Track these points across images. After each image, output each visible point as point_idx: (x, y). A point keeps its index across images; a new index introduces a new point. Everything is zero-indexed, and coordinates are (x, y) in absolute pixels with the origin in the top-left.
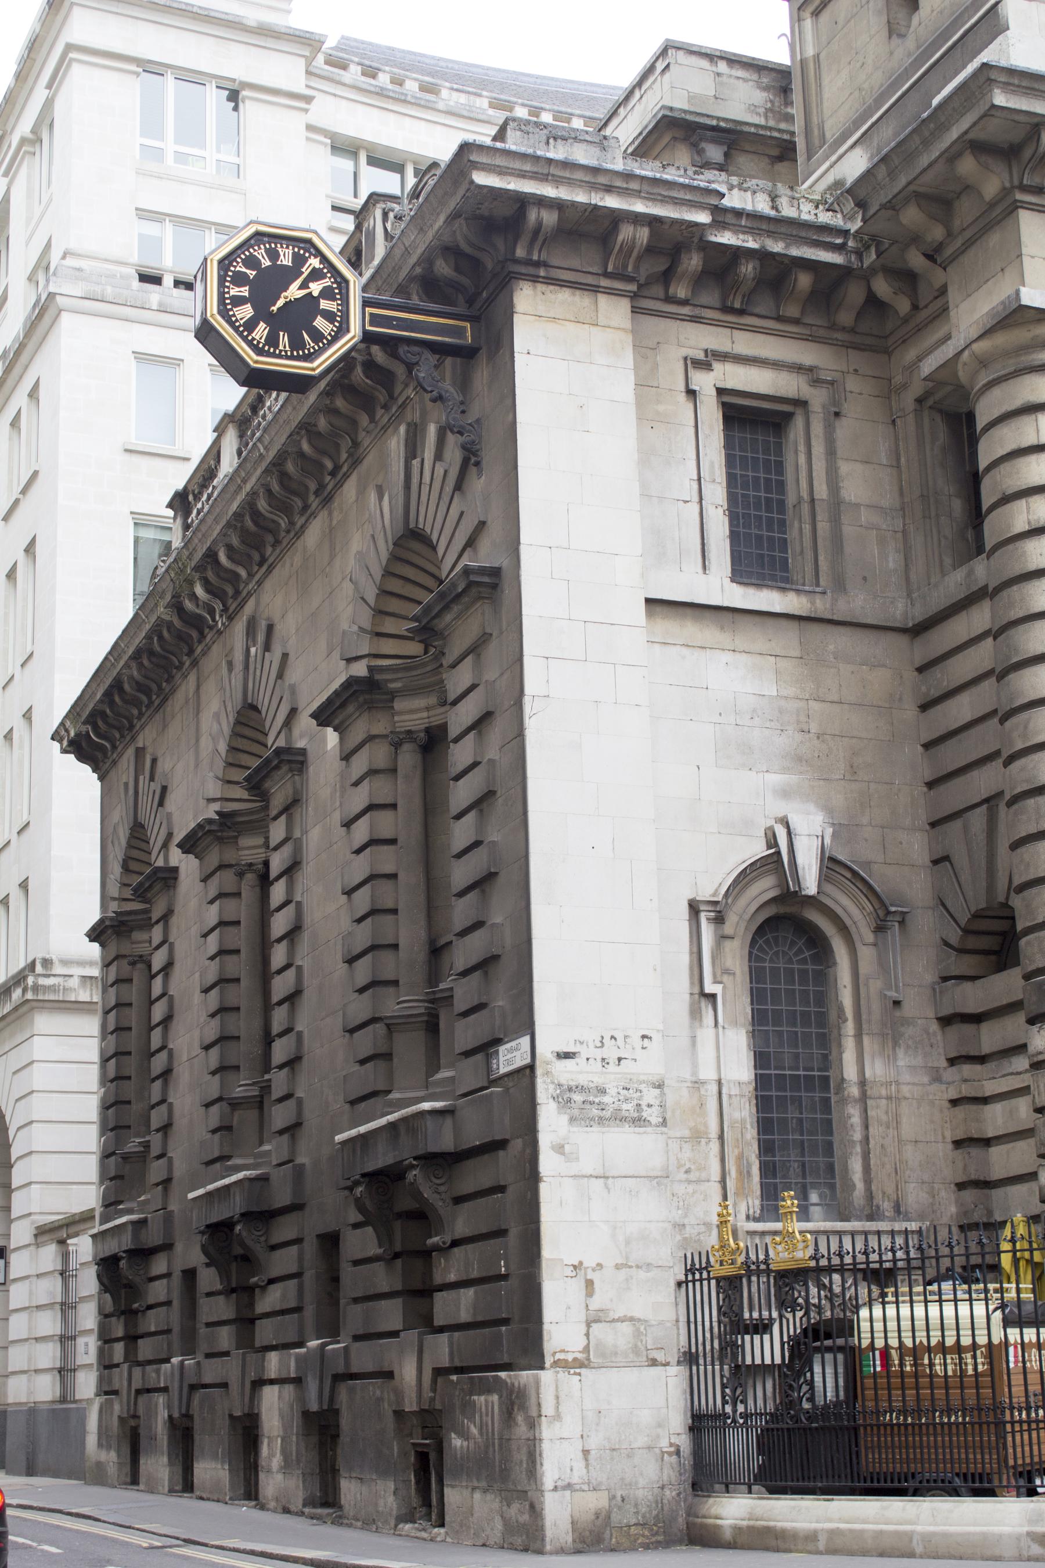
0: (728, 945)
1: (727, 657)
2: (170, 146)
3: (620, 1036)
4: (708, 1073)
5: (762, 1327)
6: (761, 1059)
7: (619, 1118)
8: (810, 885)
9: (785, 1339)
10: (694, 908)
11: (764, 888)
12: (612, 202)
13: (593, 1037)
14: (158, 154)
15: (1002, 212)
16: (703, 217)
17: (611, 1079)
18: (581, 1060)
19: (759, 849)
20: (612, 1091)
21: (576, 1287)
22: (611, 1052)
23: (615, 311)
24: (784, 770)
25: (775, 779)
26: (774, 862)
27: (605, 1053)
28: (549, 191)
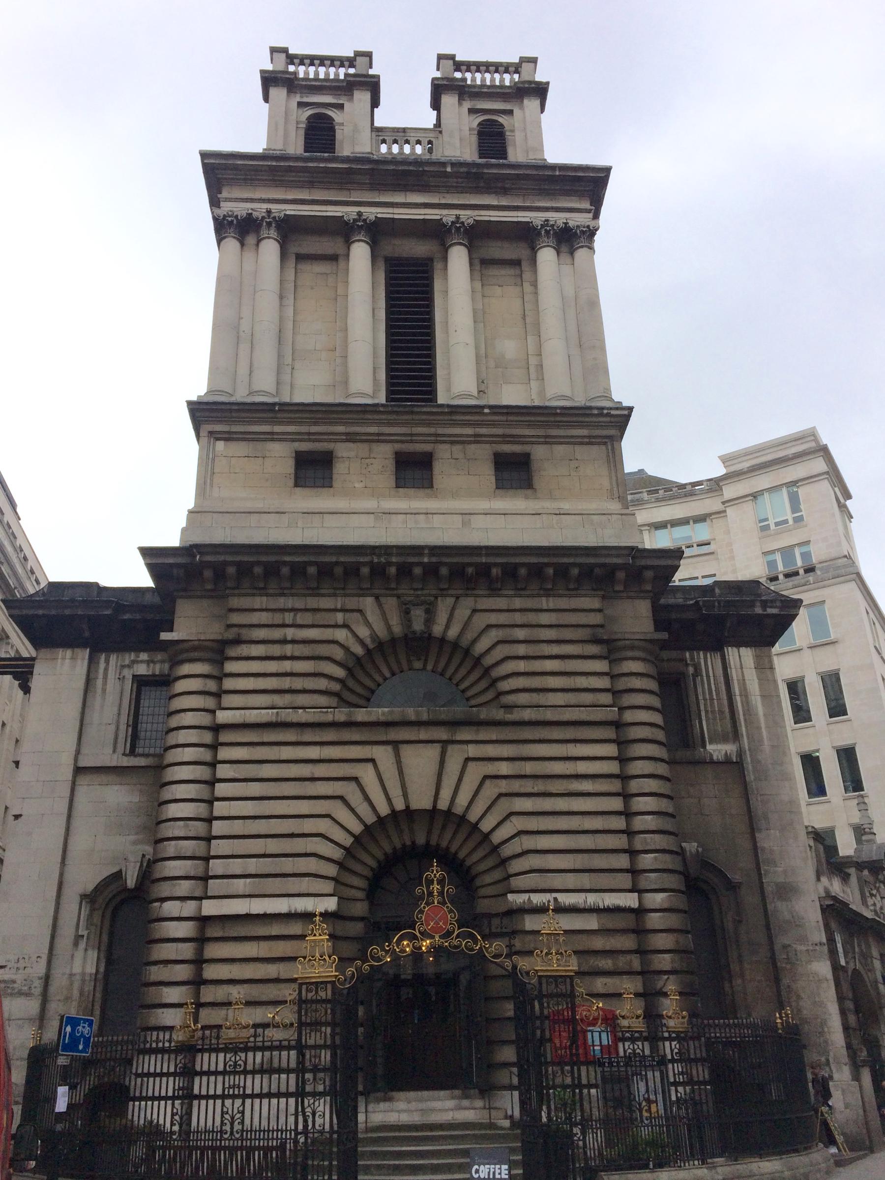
0: (96, 912)
1: (116, 788)
3: (26, 957)
9: (177, 1088)
11: (114, 888)
12: (67, 612)
13: (13, 958)
15: (174, 602)
16: (108, 612)
17: (19, 977)
18: (7, 969)
19: (115, 870)
20: (19, 982)
22: (21, 964)
24: (137, 834)
25: (132, 838)
26: (118, 876)
27: (19, 965)
28: (40, 612)
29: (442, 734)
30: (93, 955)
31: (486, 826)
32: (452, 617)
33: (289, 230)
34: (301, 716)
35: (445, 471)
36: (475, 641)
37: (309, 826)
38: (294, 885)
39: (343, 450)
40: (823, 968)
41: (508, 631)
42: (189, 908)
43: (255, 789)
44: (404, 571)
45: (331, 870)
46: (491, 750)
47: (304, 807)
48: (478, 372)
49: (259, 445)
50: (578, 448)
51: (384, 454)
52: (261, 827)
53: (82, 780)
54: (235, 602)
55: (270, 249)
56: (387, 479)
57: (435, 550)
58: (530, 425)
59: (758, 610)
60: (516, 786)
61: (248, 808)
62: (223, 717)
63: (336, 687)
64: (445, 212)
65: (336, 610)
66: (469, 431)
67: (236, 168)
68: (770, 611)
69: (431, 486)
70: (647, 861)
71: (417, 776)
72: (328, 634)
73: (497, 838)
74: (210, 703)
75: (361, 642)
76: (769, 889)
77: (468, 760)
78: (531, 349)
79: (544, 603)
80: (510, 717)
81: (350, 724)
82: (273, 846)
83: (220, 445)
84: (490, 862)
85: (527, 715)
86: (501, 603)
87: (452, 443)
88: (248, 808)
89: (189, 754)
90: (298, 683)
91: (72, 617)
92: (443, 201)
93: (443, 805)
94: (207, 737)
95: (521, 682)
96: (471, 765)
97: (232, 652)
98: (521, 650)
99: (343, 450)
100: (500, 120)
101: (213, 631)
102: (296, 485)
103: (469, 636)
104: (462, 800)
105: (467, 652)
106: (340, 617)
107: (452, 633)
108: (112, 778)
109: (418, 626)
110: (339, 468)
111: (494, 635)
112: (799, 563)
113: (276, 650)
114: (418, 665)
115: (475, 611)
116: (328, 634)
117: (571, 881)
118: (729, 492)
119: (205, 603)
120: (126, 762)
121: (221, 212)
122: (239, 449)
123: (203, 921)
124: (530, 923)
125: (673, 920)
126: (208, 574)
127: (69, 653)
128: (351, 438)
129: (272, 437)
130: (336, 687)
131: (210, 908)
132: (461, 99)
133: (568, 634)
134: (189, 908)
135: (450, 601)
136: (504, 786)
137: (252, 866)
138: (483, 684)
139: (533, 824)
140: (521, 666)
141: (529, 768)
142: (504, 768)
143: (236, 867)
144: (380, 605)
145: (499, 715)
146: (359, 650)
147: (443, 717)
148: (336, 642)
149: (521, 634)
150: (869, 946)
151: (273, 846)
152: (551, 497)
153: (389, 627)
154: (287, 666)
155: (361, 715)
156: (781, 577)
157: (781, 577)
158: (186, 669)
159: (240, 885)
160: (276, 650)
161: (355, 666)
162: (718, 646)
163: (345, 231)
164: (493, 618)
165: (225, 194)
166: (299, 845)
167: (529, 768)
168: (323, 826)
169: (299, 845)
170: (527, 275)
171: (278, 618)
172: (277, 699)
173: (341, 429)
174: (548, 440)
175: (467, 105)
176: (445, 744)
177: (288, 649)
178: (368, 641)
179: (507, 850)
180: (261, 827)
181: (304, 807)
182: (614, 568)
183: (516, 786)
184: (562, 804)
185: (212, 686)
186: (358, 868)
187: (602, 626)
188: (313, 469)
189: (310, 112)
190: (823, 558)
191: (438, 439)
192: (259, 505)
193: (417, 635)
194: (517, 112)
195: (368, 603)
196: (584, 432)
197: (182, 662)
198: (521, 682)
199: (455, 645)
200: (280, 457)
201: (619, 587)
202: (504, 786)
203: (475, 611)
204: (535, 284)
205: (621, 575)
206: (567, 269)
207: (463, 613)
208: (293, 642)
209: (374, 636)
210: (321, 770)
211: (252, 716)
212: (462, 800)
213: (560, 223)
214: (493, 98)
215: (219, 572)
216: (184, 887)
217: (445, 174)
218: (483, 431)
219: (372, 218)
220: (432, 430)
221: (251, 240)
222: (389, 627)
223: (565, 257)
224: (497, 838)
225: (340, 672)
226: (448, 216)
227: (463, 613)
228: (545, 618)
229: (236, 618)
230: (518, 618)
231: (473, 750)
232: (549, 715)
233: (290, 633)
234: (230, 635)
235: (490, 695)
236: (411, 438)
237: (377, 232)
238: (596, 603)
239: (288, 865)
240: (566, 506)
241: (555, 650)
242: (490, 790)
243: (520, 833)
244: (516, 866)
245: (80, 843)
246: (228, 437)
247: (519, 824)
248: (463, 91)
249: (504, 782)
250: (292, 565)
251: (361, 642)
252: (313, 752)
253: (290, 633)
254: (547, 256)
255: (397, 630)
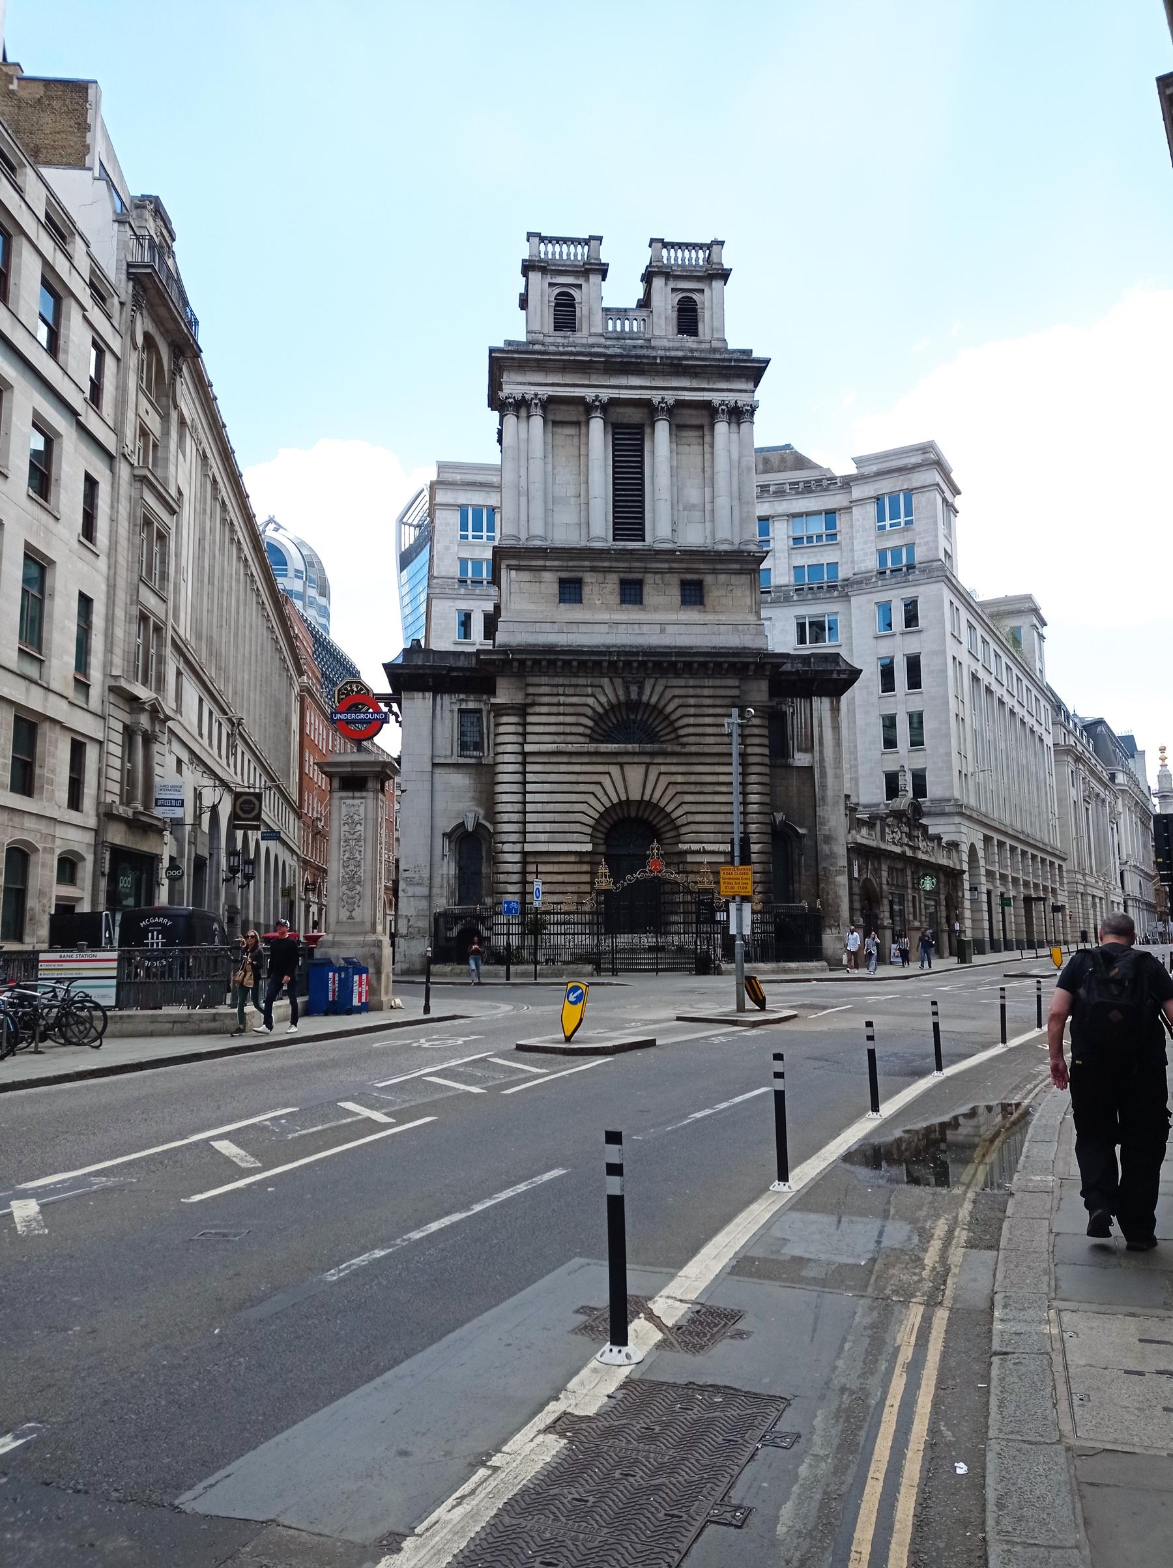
2: (470, 533)
4: (445, 872)
5: (451, 929)
6: (461, 868)
7: (418, 884)
8: (470, 828)
10: (444, 835)
14: (466, 537)
17: (416, 876)
21: (405, 921)
23: (429, 695)
29: (647, 759)
30: (453, 865)
31: (669, 809)
32: (652, 692)
33: (548, 404)
34: (570, 748)
35: (650, 595)
36: (666, 705)
37: (577, 807)
38: (569, 837)
39: (588, 578)
40: (843, 879)
41: (685, 700)
42: (518, 847)
43: (547, 787)
44: (628, 664)
45: (589, 830)
46: (673, 769)
47: (573, 797)
48: (672, 515)
49: (537, 574)
50: (733, 577)
51: (613, 580)
52: (551, 807)
53: (438, 771)
54: (531, 680)
55: (537, 422)
56: (615, 599)
57: (645, 654)
58: (704, 562)
59: (835, 676)
60: (686, 788)
61: (545, 797)
62: (528, 748)
63: (588, 732)
64: (654, 392)
65: (587, 686)
66: (666, 565)
67: (513, 359)
68: (843, 676)
69: (641, 603)
70: (753, 828)
71: (633, 782)
72: (583, 700)
73: (674, 816)
74: (520, 739)
75: (602, 705)
76: (820, 838)
77: (660, 774)
78: (708, 498)
79: (707, 682)
80: (683, 750)
81: (597, 753)
82: (558, 817)
83: (513, 573)
84: (669, 827)
85: (694, 749)
86: (682, 682)
87: (656, 573)
88: (545, 797)
89: (511, 768)
90: (568, 729)
91: (425, 674)
92: (654, 384)
93: (647, 798)
94: (519, 758)
95: (691, 730)
96: (662, 777)
97: (530, 710)
98: (692, 711)
99: (588, 578)
100: (694, 297)
101: (519, 699)
102: (562, 600)
103: (662, 703)
104: (657, 795)
105: (661, 712)
106: (589, 690)
107: (653, 700)
108: (451, 770)
109: (634, 696)
110: (586, 590)
111: (677, 702)
112: (904, 561)
113: (554, 709)
114: (632, 717)
115: (666, 687)
116: (583, 700)
117: (712, 837)
118: (857, 492)
119: (513, 680)
120: (462, 761)
121: (502, 395)
122: (525, 576)
123: (525, 854)
124: (690, 858)
125: (763, 858)
126: (515, 664)
127: (420, 695)
128: (593, 569)
129: (545, 569)
130: (588, 732)
131: (528, 848)
132: (667, 279)
133: (719, 702)
134: (518, 847)
135: (652, 681)
136: (679, 788)
137: (548, 827)
138: (669, 729)
139: (694, 808)
140: (692, 720)
141: (693, 778)
142: (680, 779)
143: (539, 827)
144: (612, 682)
145: (678, 749)
146: (600, 710)
147: (647, 750)
148: (588, 705)
149: (692, 701)
150: (880, 864)
151: (558, 817)
152: (715, 612)
153: (617, 696)
154: (561, 719)
155: (603, 747)
156: (888, 572)
157: (888, 572)
158: (505, 719)
159: (543, 837)
160: (554, 709)
161: (598, 718)
162: (808, 695)
163: (587, 408)
164: (677, 692)
165: (505, 378)
166: (571, 817)
167: (693, 778)
168: (583, 807)
169: (571, 817)
170: (707, 439)
171: (555, 691)
172: (557, 739)
173: (587, 563)
174: (715, 572)
175: (672, 284)
176: (648, 764)
177: (561, 709)
178: (606, 705)
179: (679, 822)
180: (551, 807)
181: (573, 797)
182: (748, 664)
183: (686, 788)
184: (709, 798)
185: (520, 729)
186: (600, 828)
187: (738, 697)
188: (570, 591)
189: (558, 291)
190: (923, 559)
191: (646, 571)
192: (540, 617)
193: (634, 701)
194: (707, 290)
195: (606, 680)
196: (737, 566)
197: (503, 715)
198: (691, 730)
199: (655, 707)
200: (550, 580)
201: (751, 673)
202: (679, 788)
203: (666, 687)
204: (712, 446)
205: (752, 667)
206: (734, 436)
207: (659, 689)
208: (564, 705)
209: (609, 701)
210: (582, 778)
211: (544, 748)
212: (657, 795)
213: (732, 403)
214: (690, 278)
215: (522, 663)
216: (514, 837)
217: (656, 364)
218: (675, 565)
219: (606, 399)
220: (643, 565)
221: (523, 413)
222: (617, 696)
223: (734, 427)
224: (674, 816)
225: (590, 723)
226: (655, 396)
227: (659, 689)
228: (706, 692)
229: (531, 690)
230: (691, 692)
231: (663, 769)
232: (706, 749)
233: (562, 699)
234: (529, 701)
235: (673, 736)
236: (630, 570)
237: (607, 407)
238: (736, 683)
239: (566, 827)
240: (722, 618)
241: (711, 711)
242: (672, 791)
243: (686, 813)
244: (683, 830)
245: (440, 805)
246: (518, 568)
247: (686, 808)
248: (667, 274)
249: (679, 786)
250: (564, 661)
251: (602, 705)
252: (577, 768)
253: (562, 699)
254: (721, 428)
255: (622, 698)
